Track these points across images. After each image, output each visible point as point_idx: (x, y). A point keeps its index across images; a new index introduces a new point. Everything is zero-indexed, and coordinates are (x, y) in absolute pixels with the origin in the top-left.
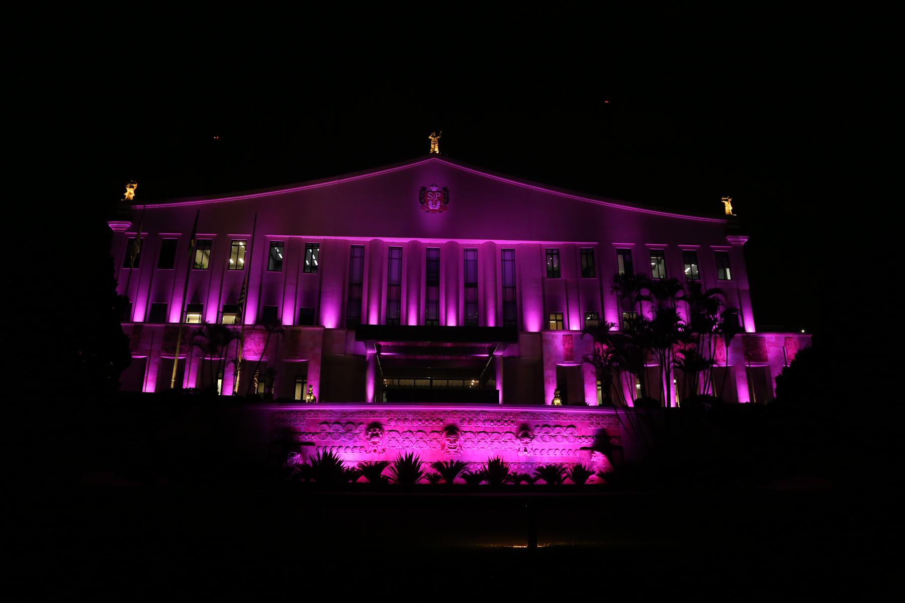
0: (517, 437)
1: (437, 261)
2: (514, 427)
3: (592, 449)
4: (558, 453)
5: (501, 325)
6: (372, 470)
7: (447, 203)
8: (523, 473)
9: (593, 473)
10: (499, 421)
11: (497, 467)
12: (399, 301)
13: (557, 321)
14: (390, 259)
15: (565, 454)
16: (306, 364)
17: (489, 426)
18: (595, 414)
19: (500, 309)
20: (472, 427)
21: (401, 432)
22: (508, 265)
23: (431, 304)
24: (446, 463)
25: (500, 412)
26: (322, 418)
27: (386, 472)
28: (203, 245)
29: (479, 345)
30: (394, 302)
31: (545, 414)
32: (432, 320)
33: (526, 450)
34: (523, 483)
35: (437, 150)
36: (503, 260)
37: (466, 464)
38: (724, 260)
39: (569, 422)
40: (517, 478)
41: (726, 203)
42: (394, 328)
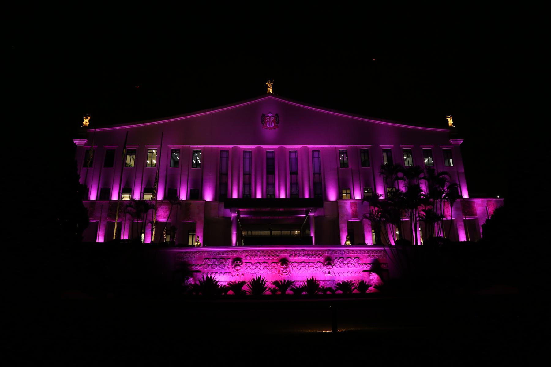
0: (324, 265)
1: (273, 158)
2: (322, 259)
3: (370, 271)
4: (349, 274)
5: (313, 197)
6: (236, 287)
7: (278, 123)
8: (328, 286)
9: (371, 286)
10: (313, 255)
11: (312, 283)
12: (250, 184)
13: (347, 194)
14: (244, 158)
15: (353, 275)
16: (194, 224)
17: (307, 258)
18: (371, 250)
19: (312, 187)
20: (297, 259)
21: (253, 263)
22: (316, 160)
23: (270, 185)
24: (281, 281)
25: (313, 250)
26: (205, 256)
27: (245, 288)
28: (131, 153)
29: (300, 209)
30: (247, 184)
31: (341, 251)
32: (271, 195)
33: (329, 273)
34: (328, 293)
35: (271, 91)
36: (313, 158)
37: (293, 282)
38: (448, 154)
39: (356, 255)
40: (324, 290)
41: (449, 119)
42: (246, 200)
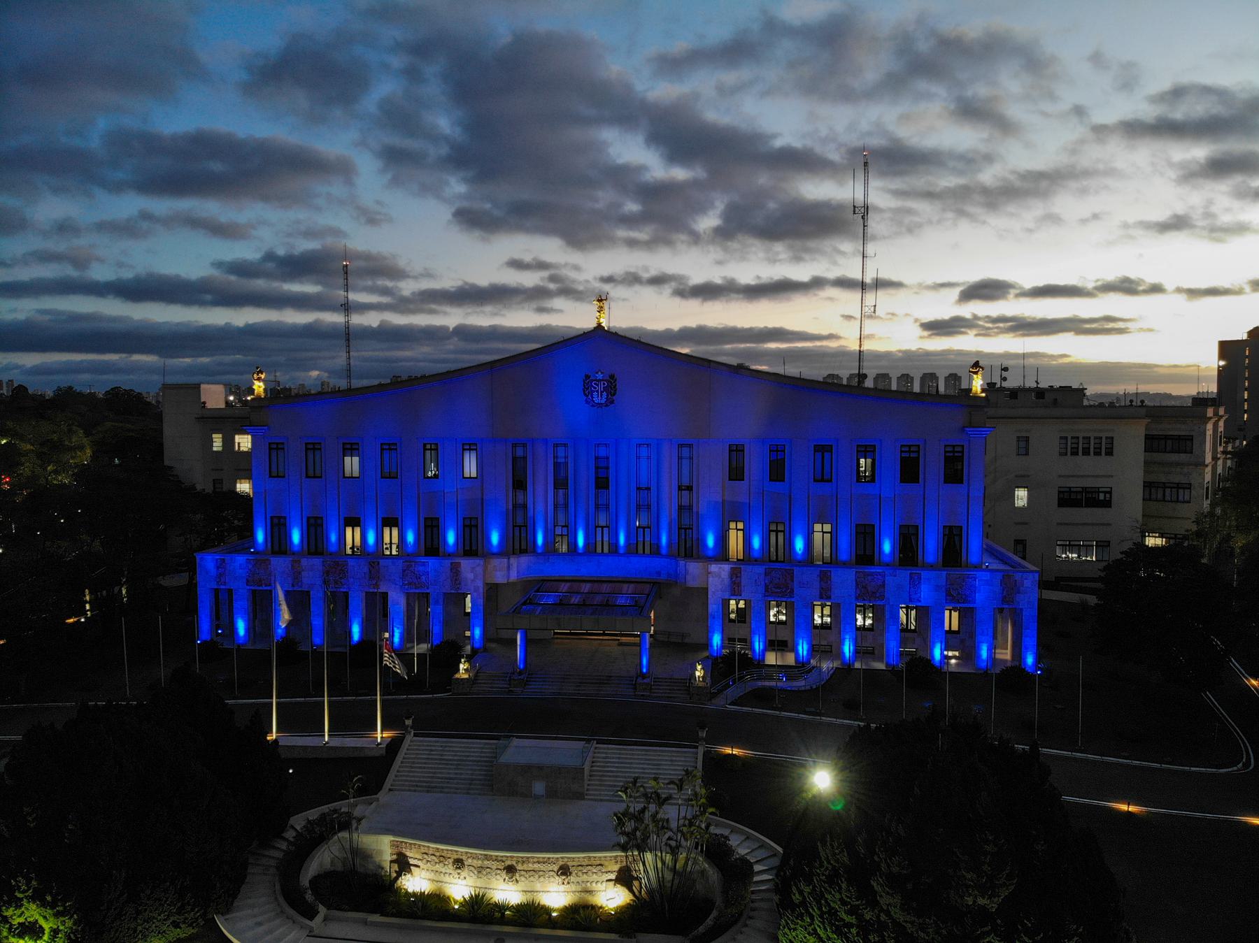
12: (566, 505)
17: (536, 866)
20: (525, 867)
